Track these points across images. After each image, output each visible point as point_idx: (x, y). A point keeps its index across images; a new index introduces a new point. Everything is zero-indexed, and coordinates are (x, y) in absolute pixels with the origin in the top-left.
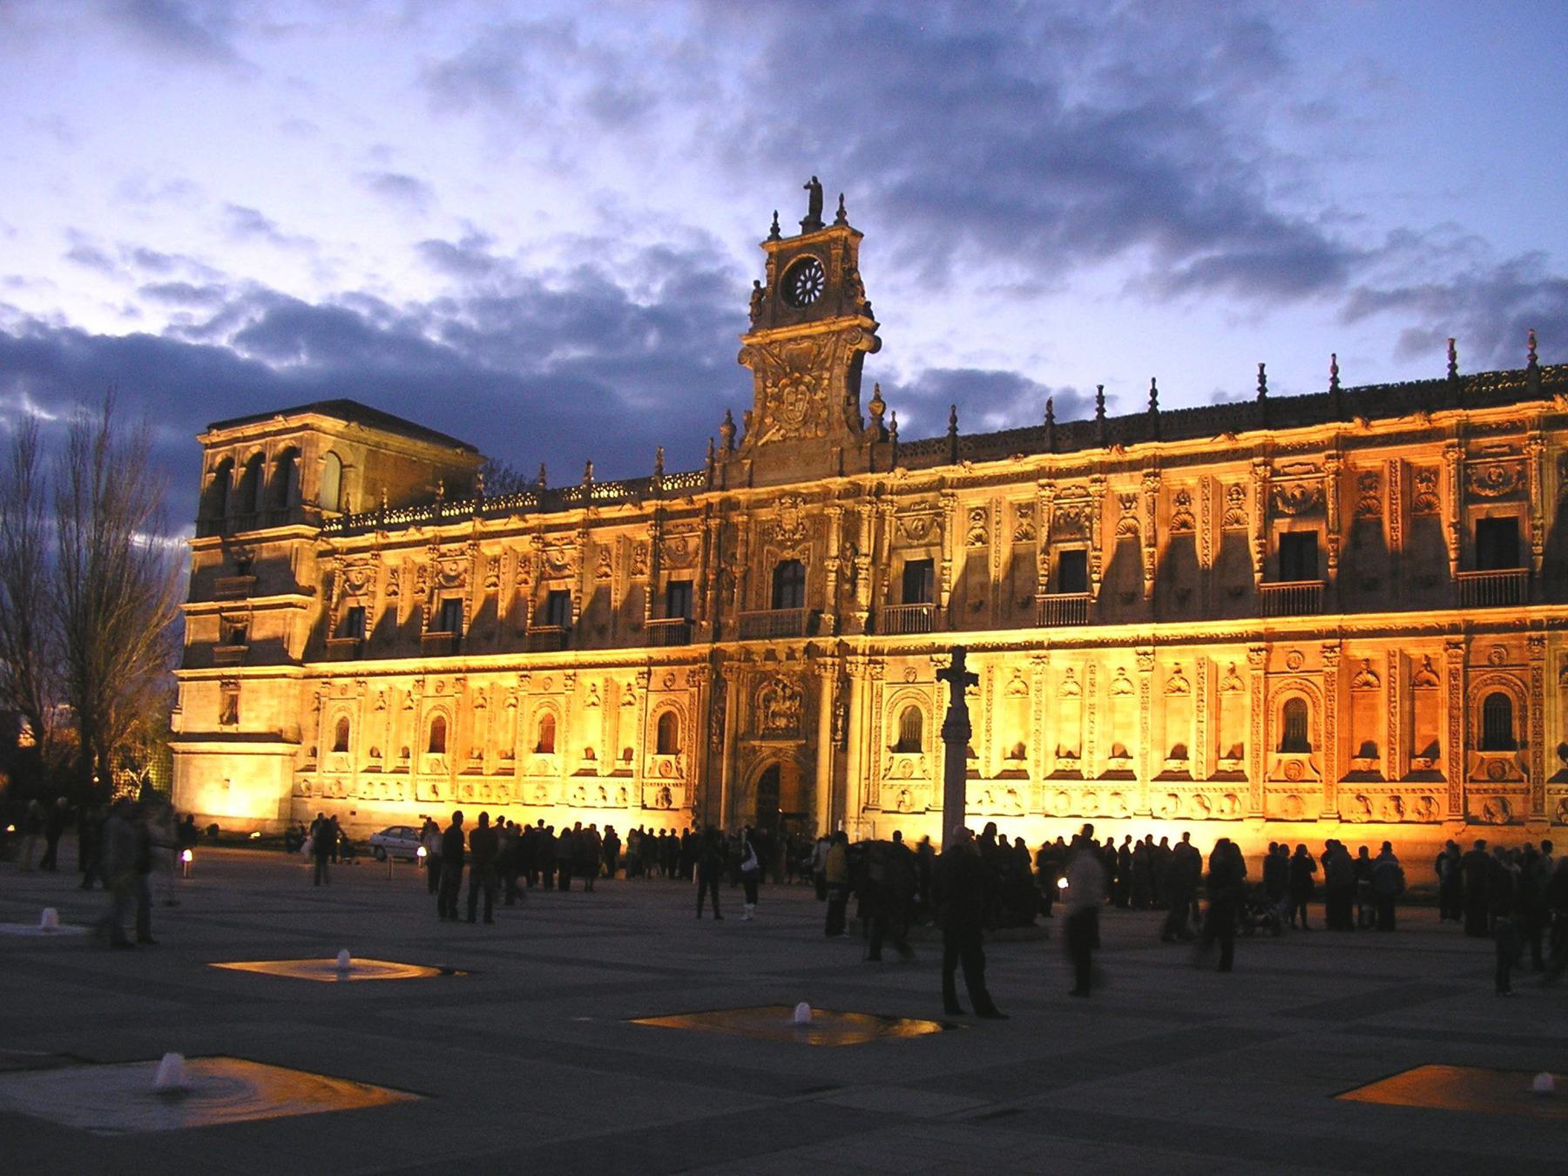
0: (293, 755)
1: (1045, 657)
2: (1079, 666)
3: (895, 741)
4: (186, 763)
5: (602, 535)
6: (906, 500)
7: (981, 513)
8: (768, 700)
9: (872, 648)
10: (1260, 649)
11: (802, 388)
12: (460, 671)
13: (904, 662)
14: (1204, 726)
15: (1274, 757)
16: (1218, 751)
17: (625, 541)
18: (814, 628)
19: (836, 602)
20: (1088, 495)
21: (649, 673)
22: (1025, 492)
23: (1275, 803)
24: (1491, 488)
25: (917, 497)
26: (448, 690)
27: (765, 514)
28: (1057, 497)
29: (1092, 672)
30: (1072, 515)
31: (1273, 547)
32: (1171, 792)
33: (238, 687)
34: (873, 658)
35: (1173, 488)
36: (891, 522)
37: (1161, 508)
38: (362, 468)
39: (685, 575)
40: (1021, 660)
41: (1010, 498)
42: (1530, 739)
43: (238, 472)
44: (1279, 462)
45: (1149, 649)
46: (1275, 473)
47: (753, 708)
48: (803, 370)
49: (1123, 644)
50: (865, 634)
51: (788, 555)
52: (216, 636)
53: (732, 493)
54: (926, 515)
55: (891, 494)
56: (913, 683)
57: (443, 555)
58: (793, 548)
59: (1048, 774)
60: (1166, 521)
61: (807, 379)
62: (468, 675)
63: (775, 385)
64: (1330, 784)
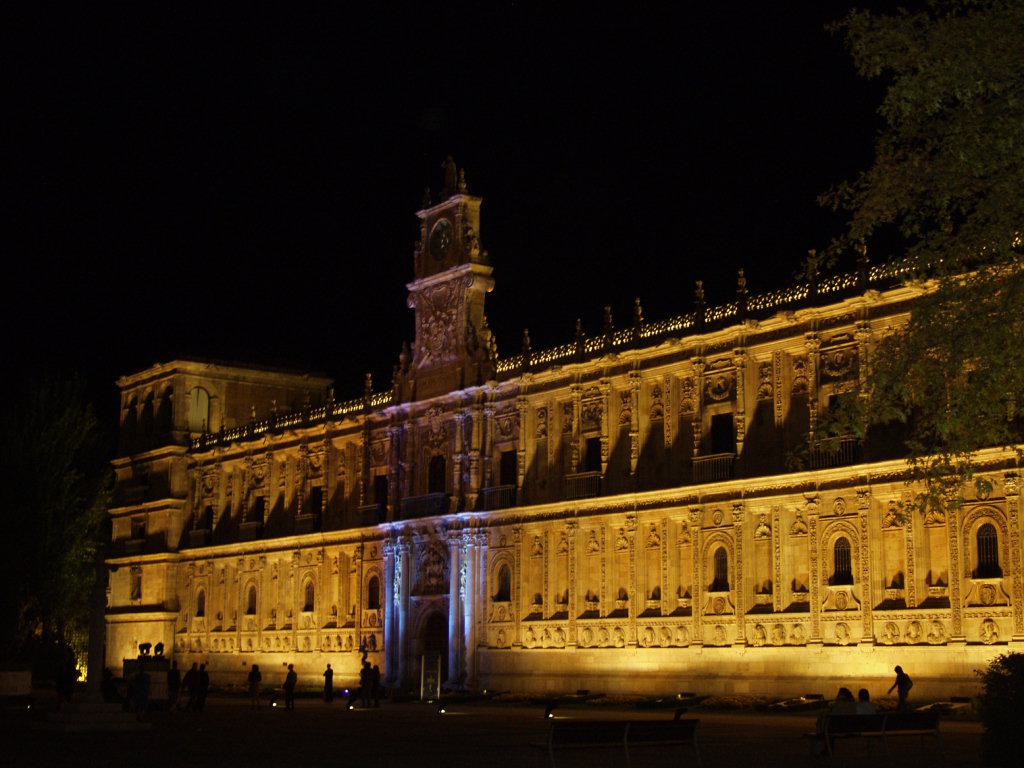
0: (175, 620)
2: (597, 527)
3: (495, 593)
4: (114, 630)
5: (339, 443)
6: (499, 405)
7: (543, 412)
11: (441, 323)
13: (499, 531)
17: (350, 445)
19: (461, 487)
20: (600, 394)
21: (362, 547)
22: (563, 395)
24: (837, 369)
26: (256, 567)
27: (423, 421)
28: (584, 397)
29: (603, 533)
33: (141, 571)
38: (224, 398)
39: (383, 470)
40: (559, 525)
41: (558, 399)
42: (861, 576)
51: (434, 452)
52: (129, 533)
53: (403, 405)
55: (491, 401)
57: (255, 463)
58: (438, 446)
59: (580, 614)
62: (267, 554)
63: (426, 322)
64: (740, 616)
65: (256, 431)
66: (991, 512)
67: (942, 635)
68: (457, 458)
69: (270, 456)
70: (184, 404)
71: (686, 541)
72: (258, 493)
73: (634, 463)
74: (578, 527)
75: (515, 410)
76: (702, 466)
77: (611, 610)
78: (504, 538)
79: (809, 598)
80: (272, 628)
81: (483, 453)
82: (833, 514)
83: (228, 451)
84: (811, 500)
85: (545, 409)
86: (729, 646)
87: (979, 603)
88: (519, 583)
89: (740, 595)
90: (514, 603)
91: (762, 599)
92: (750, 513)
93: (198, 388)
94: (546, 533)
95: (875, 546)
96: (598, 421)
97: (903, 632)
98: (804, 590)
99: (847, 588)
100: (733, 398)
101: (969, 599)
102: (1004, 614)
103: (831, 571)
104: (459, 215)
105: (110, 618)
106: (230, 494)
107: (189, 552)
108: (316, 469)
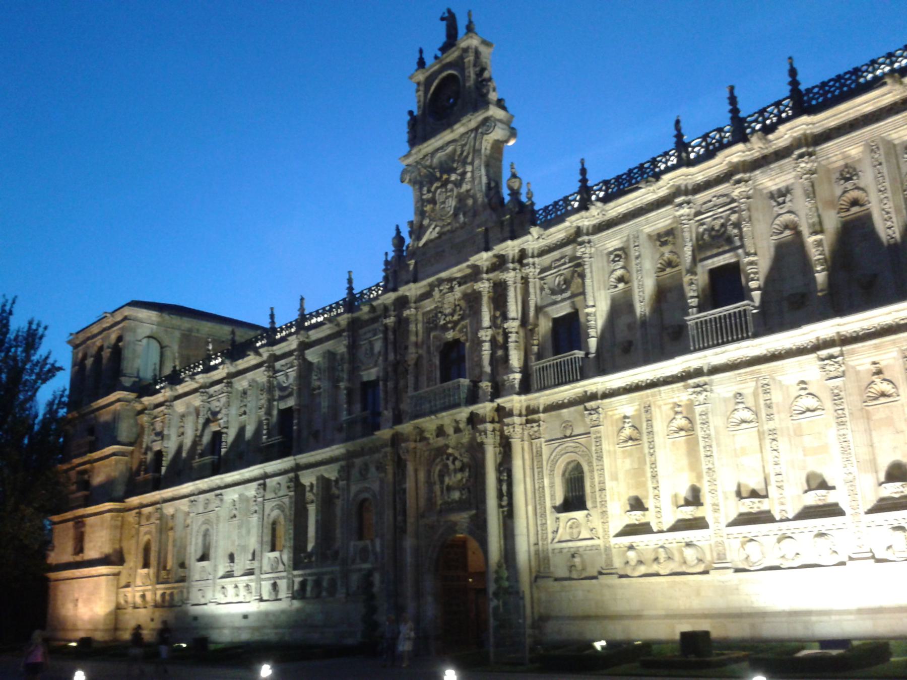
0: (117, 574)
1: (706, 384)
2: (748, 388)
3: (559, 500)
6: (547, 259)
7: (621, 254)
8: (441, 476)
9: (528, 408)
11: (450, 186)
12: (220, 488)
13: (559, 416)
17: (331, 355)
18: (473, 397)
19: (492, 370)
20: (733, 201)
22: (660, 220)
25: (556, 254)
26: (211, 507)
29: (766, 392)
30: (717, 228)
32: (896, 525)
33: (83, 524)
34: (529, 417)
35: (831, 166)
36: (535, 284)
37: (823, 191)
38: (175, 347)
39: (371, 374)
40: (679, 394)
41: (648, 229)
43: (89, 362)
45: (835, 351)
47: (430, 484)
49: (801, 351)
51: (450, 335)
55: (533, 257)
56: (570, 437)
57: (211, 396)
58: (453, 328)
59: (730, 519)
60: (831, 204)
61: (453, 177)
63: (429, 191)
65: (212, 363)
69: (229, 384)
70: (134, 351)
72: (214, 427)
73: (821, 277)
74: (711, 391)
80: (229, 575)
81: (524, 322)
83: (181, 389)
90: (595, 514)
93: (149, 337)
105: (53, 575)
106: (183, 434)
107: (135, 500)
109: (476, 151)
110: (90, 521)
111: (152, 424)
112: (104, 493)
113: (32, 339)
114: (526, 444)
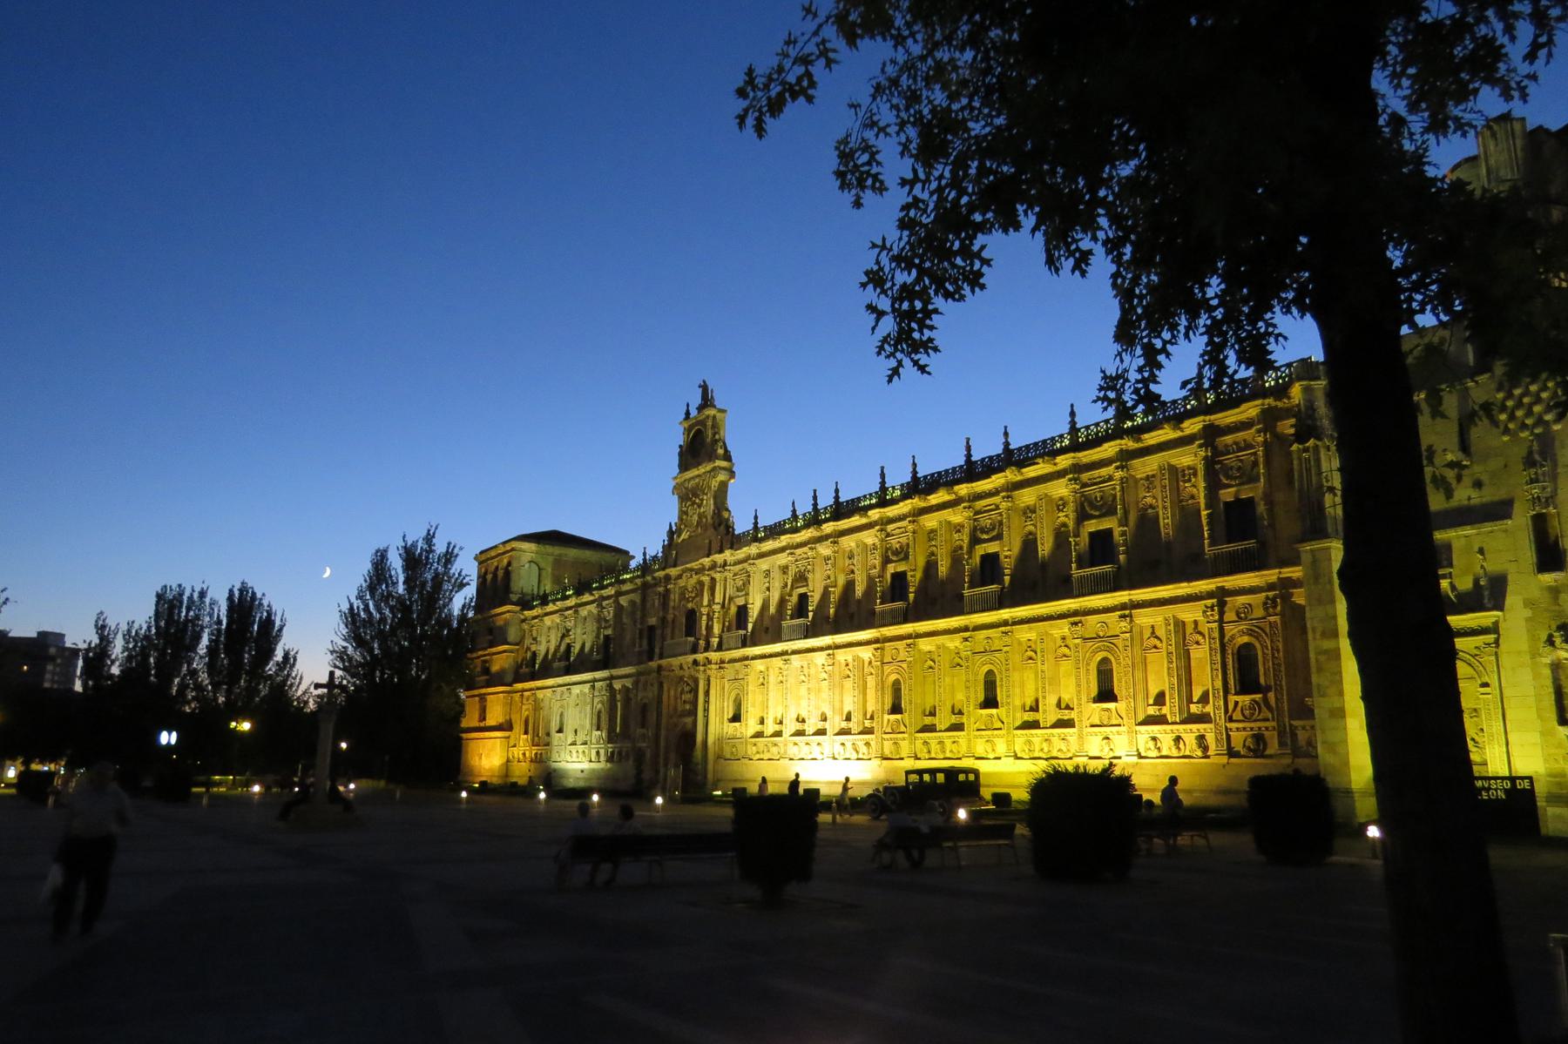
0: (508, 737)
7: (767, 573)
8: (681, 694)
10: (878, 649)
12: (569, 684)
14: (856, 699)
15: (886, 717)
16: (865, 714)
18: (695, 650)
23: (888, 748)
24: (987, 533)
26: (564, 697)
28: (796, 561)
31: (887, 582)
37: (840, 563)
38: (550, 570)
39: (653, 621)
43: (489, 577)
44: (890, 527)
46: (888, 535)
47: (676, 698)
48: (696, 495)
49: (821, 649)
50: (715, 651)
51: (690, 606)
53: (668, 571)
54: (744, 577)
55: (730, 565)
57: (566, 618)
59: (792, 733)
64: (910, 734)
65: (567, 593)
66: (1108, 647)
67: (1068, 750)
68: (704, 610)
69: (576, 612)
70: (519, 574)
71: (872, 674)
72: (567, 640)
74: (791, 664)
75: (747, 572)
76: (883, 613)
77: (815, 730)
78: (737, 672)
79: (964, 720)
80: (574, 744)
81: (723, 606)
82: (983, 650)
84: (966, 639)
85: (769, 571)
86: (902, 759)
87: (1099, 723)
88: (747, 708)
89: (910, 717)
90: (743, 723)
91: (928, 720)
92: (919, 650)
93: (530, 562)
94: (768, 668)
95: (1016, 676)
96: (806, 579)
97: (1037, 749)
98: (961, 713)
99: (994, 711)
100: (906, 558)
101: (1090, 720)
102: (1119, 733)
103: (981, 698)
104: (710, 423)
105: (464, 736)
107: (519, 686)
108: (606, 621)
109: (710, 488)
110: (488, 697)
111: (531, 631)
112: (496, 680)
113: (449, 557)
114: (718, 681)
